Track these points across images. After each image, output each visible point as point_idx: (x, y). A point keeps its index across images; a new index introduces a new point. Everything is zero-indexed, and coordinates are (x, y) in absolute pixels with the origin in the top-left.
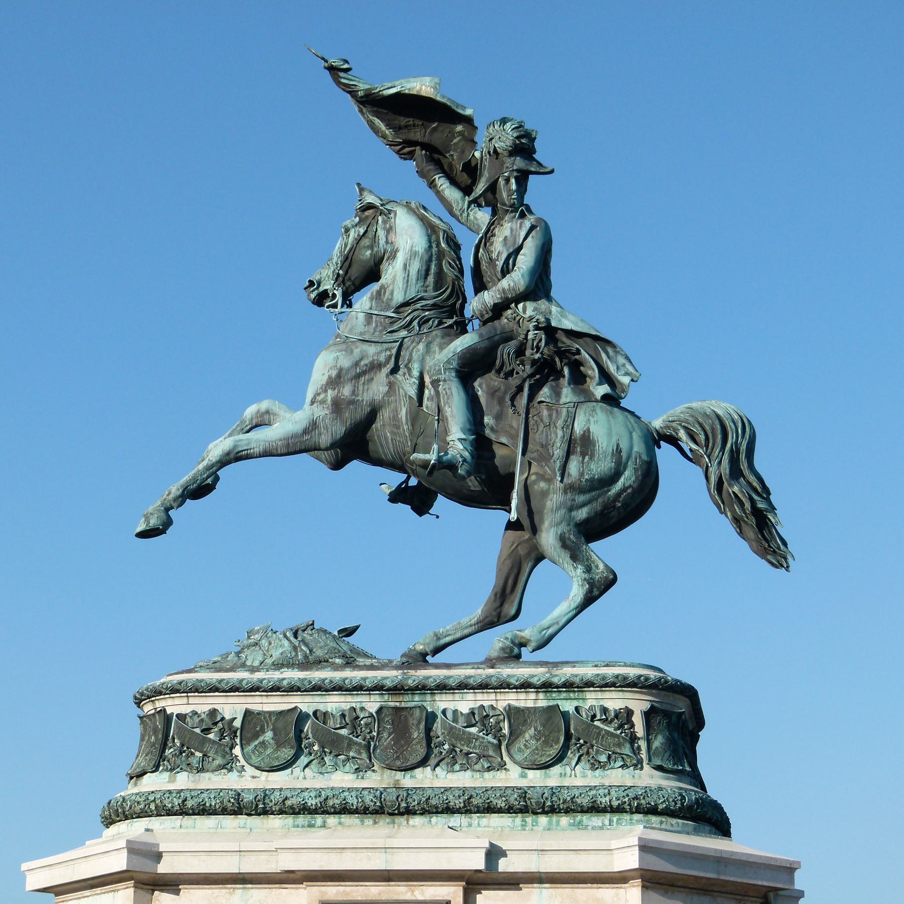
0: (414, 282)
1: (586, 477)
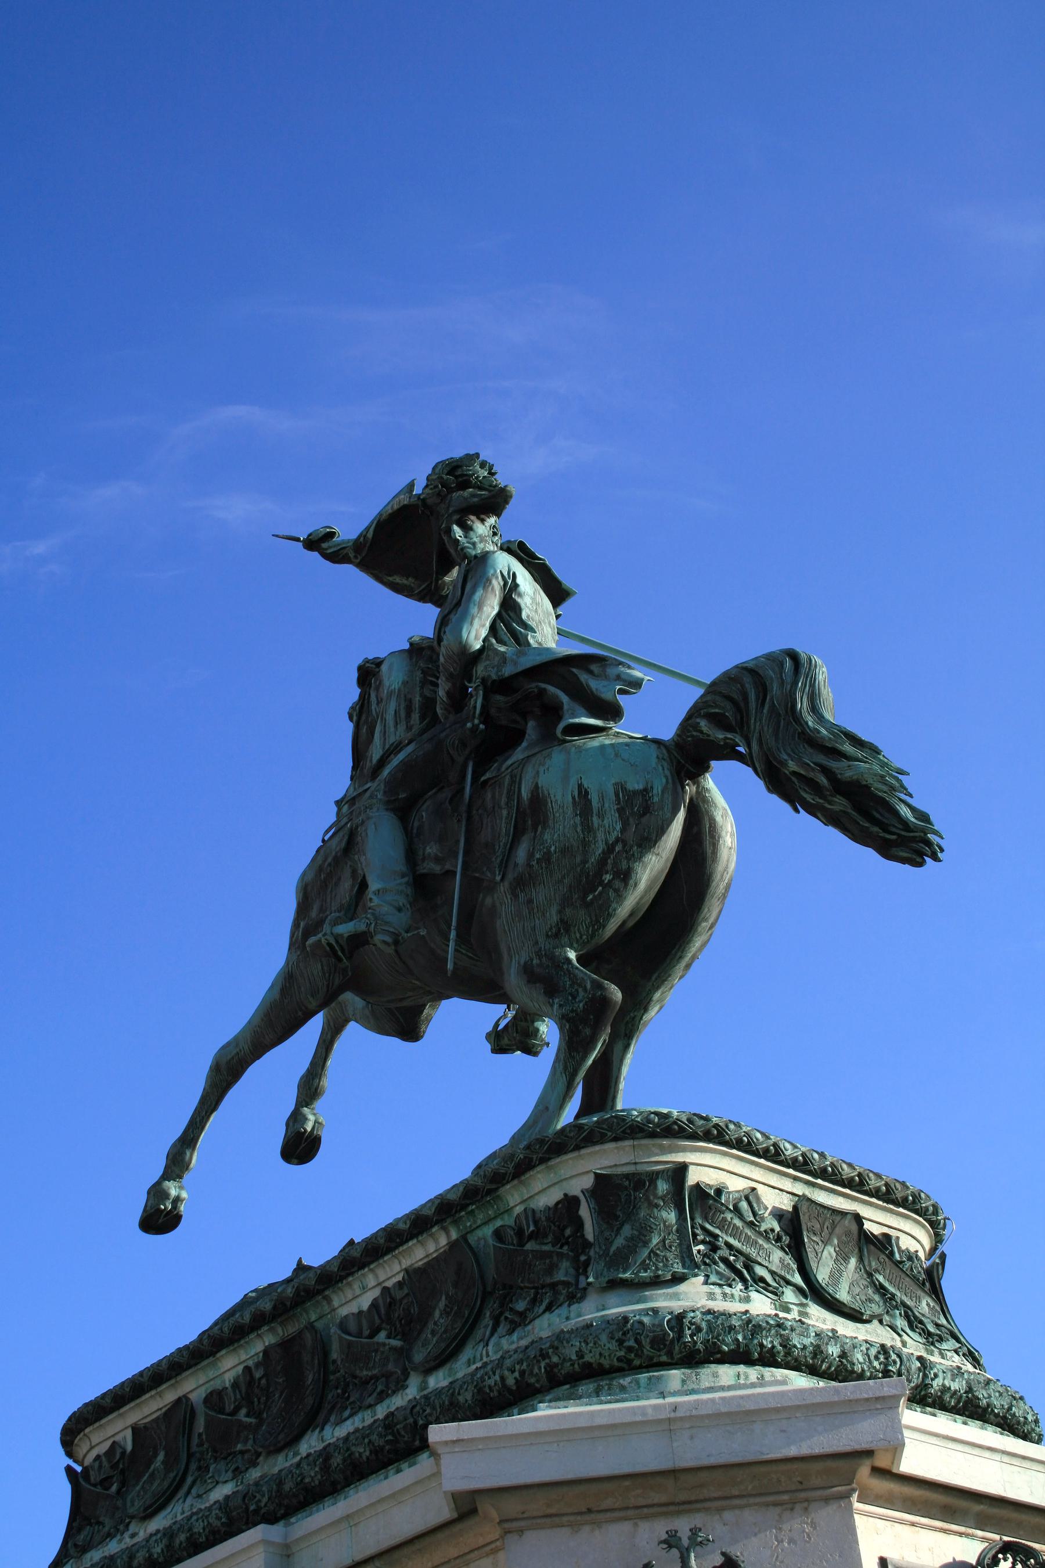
0: (392, 729)
1: (538, 856)
